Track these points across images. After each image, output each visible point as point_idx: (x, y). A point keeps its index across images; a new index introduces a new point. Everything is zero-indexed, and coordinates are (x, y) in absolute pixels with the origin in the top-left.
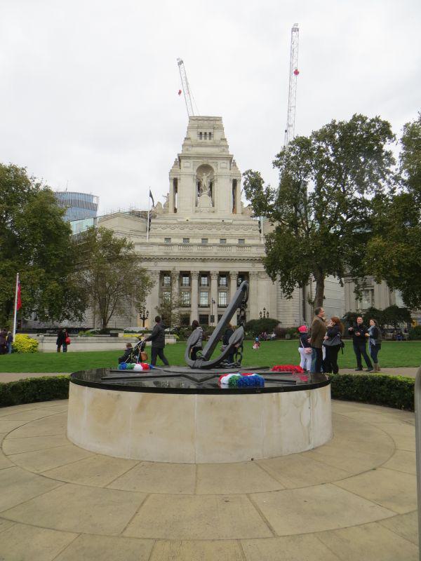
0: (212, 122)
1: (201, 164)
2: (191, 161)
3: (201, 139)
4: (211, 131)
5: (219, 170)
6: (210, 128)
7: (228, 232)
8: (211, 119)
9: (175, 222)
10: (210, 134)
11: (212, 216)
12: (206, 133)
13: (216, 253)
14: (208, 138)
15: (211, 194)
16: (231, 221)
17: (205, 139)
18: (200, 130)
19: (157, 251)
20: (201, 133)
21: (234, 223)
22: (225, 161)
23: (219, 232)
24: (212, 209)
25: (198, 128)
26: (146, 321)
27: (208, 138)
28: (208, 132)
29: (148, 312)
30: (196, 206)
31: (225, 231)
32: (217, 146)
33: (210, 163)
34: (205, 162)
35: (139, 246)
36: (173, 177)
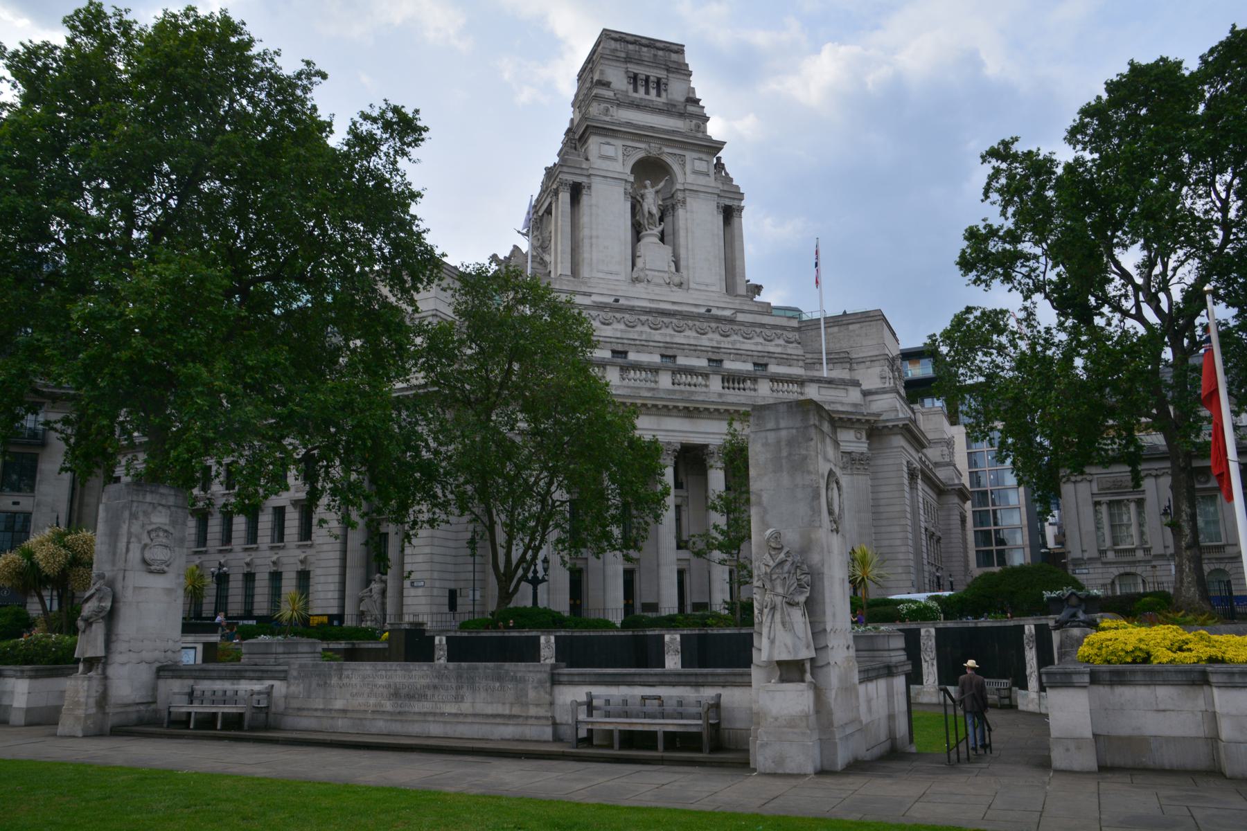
0: (660, 53)
1: (641, 155)
2: (619, 143)
3: (636, 90)
4: (662, 74)
5: (691, 178)
7: (726, 343)
8: (658, 45)
11: (678, 295)
13: (720, 395)
14: (653, 92)
16: (727, 313)
17: (647, 92)
18: (634, 68)
21: (741, 317)
22: (704, 156)
23: (705, 341)
24: (677, 279)
25: (628, 60)
26: (542, 588)
28: (654, 73)
30: (634, 265)
31: (717, 337)
32: (682, 115)
33: (668, 154)
34: (654, 149)
36: (572, 178)
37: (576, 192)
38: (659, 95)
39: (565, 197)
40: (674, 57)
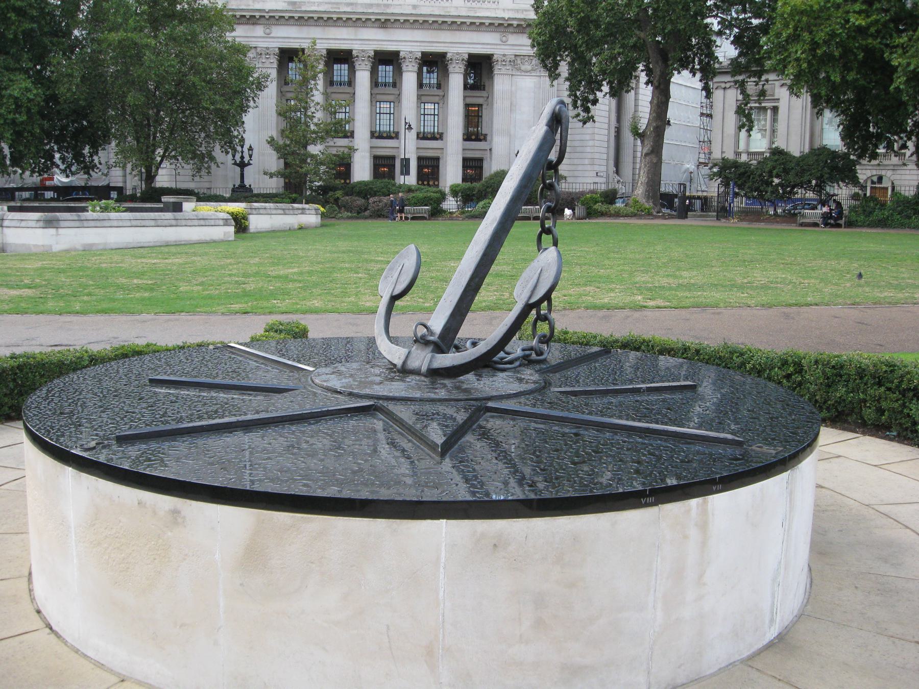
26: (246, 169)
29: (251, 149)
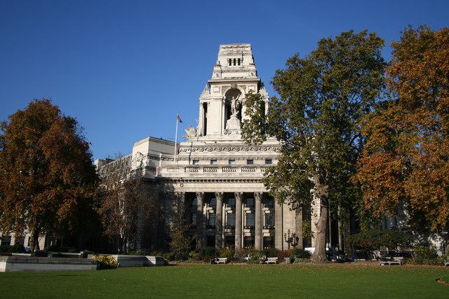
2: (221, 86)
3: (230, 65)
4: (240, 57)
6: (238, 53)
9: (203, 144)
10: (239, 60)
12: (235, 59)
13: (240, 174)
14: (237, 64)
15: (239, 116)
17: (235, 65)
18: (230, 57)
19: (181, 174)
20: (230, 60)
22: (254, 84)
27: (237, 64)
28: (237, 57)
35: (166, 169)
37: (205, 105)
38: (239, 65)
39: (201, 108)
40: (246, 49)
